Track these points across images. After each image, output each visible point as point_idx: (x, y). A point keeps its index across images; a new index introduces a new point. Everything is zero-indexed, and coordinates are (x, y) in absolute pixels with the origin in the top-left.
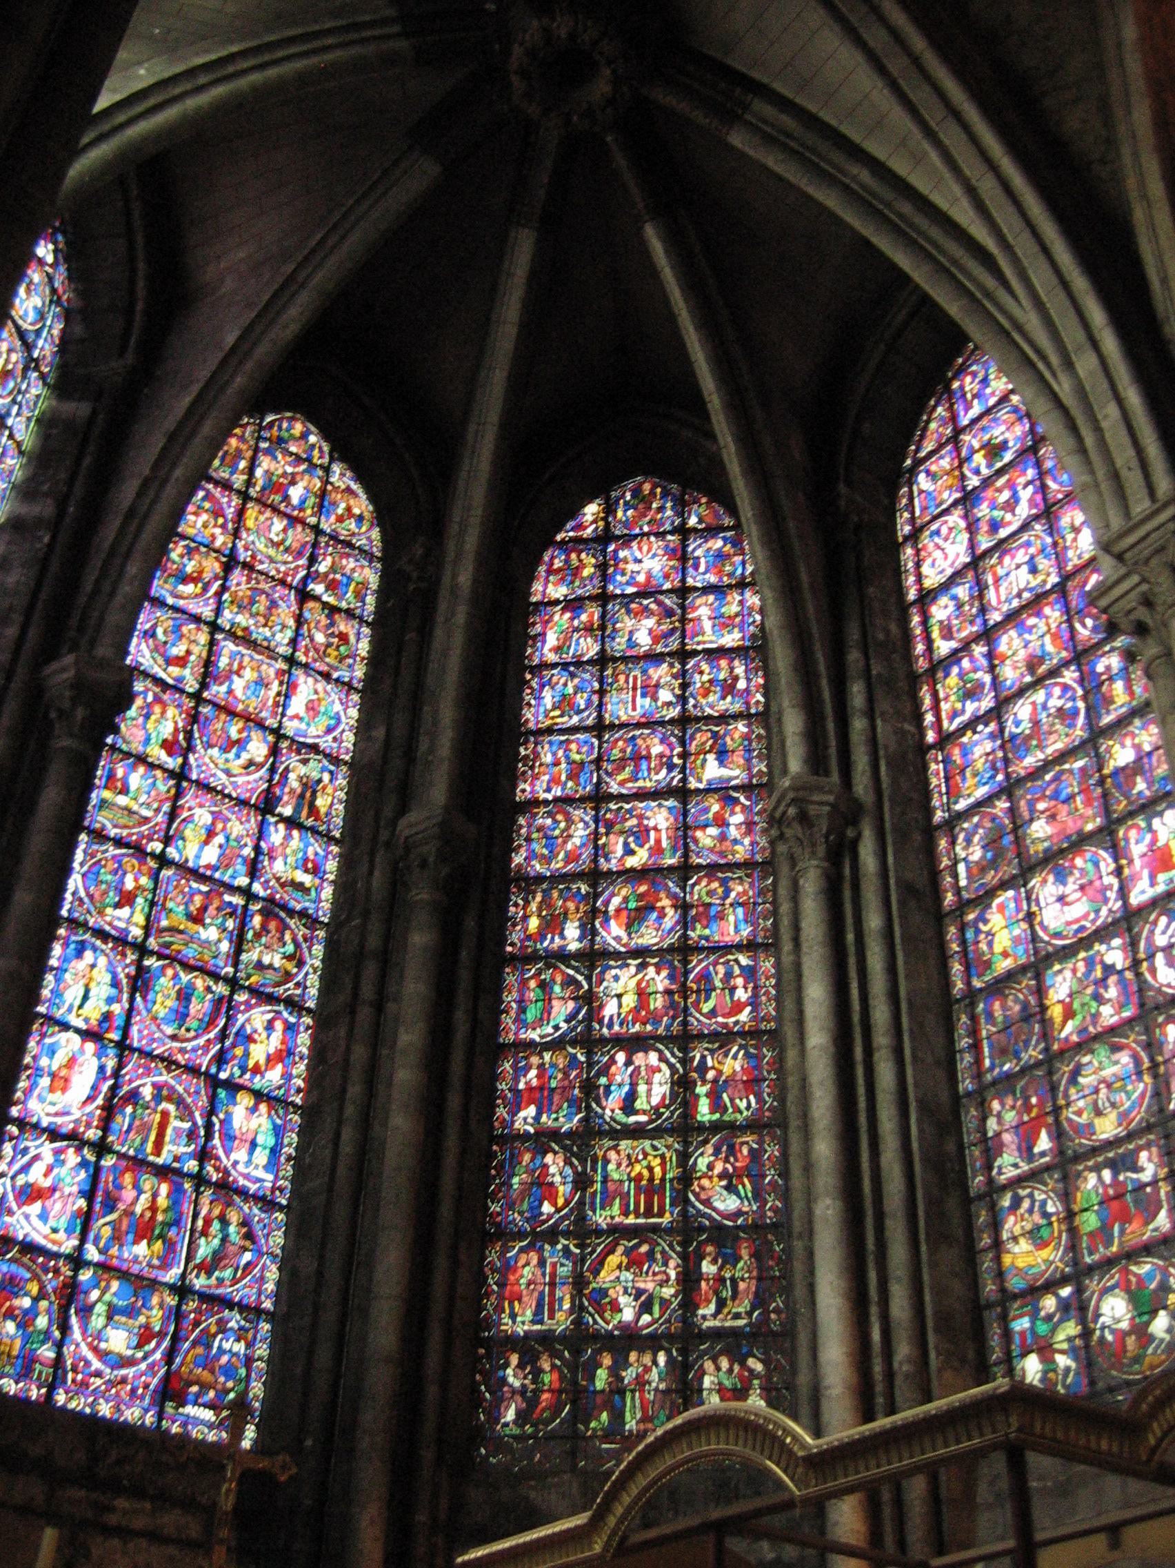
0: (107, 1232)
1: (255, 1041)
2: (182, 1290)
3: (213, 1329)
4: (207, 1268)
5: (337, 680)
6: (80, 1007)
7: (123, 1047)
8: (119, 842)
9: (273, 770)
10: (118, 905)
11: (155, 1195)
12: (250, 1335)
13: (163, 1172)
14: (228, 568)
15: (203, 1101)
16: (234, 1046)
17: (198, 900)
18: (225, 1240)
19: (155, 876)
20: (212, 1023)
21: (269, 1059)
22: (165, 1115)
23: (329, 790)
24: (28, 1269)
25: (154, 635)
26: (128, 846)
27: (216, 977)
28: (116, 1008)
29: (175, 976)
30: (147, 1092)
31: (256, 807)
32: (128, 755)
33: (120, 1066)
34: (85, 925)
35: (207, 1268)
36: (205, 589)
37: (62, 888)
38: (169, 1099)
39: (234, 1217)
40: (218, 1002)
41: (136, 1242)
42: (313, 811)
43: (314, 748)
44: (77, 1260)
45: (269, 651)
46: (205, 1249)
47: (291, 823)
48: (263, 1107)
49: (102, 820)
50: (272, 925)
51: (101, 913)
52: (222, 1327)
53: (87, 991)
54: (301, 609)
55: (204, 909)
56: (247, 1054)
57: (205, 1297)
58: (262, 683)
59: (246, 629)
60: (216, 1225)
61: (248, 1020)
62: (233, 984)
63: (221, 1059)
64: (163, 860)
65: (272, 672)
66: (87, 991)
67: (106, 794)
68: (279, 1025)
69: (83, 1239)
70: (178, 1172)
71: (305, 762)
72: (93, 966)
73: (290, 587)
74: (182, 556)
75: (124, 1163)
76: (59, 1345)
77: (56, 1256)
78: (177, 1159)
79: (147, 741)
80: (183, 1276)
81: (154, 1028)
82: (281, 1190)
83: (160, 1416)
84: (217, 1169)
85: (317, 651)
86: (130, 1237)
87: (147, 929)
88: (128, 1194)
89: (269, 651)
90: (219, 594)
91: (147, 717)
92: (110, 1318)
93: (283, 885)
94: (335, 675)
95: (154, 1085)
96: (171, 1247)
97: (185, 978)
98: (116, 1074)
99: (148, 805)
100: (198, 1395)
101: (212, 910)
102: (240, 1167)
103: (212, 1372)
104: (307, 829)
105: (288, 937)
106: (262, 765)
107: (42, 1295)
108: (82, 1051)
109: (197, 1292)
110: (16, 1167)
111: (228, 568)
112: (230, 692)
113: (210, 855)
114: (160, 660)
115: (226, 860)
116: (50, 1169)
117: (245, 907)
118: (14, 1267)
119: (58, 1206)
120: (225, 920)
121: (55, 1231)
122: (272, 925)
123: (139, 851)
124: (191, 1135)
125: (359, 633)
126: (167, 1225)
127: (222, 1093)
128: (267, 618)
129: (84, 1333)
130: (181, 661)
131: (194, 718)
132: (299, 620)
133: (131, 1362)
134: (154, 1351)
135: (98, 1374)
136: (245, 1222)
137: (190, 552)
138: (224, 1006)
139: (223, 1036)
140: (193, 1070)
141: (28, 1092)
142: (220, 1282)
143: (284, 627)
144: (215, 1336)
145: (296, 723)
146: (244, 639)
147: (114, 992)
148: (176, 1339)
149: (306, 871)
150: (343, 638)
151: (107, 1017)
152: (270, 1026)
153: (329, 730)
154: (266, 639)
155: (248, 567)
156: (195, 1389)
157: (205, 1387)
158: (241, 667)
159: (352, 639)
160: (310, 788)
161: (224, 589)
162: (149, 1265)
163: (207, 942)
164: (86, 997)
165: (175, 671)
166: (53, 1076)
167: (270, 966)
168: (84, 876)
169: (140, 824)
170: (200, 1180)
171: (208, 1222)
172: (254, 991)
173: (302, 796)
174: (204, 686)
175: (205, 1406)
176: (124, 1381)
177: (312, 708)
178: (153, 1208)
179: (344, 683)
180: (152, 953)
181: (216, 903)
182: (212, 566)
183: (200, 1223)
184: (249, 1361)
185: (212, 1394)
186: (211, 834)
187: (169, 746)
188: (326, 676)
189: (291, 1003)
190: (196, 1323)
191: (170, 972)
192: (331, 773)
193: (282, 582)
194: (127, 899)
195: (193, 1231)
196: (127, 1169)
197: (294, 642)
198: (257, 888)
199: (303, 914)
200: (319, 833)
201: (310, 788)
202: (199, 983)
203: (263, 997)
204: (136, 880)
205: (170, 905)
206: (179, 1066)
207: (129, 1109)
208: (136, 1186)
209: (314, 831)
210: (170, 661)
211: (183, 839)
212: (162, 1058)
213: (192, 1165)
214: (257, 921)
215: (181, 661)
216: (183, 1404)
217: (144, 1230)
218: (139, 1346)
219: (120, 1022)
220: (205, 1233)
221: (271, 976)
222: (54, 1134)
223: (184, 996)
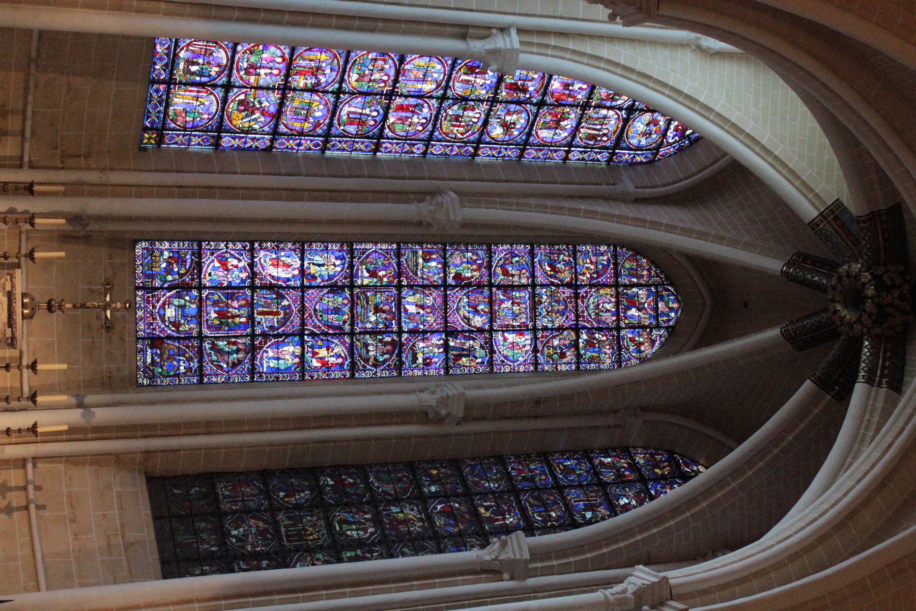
0: (216, 297)
1: (328, 350)
2: (201, 337)
3: (187, 355)
4: (214, 347)
5: (536, 357)
6: (314, 264)
7: (303, 288)
8: (399, 264)
9: (471, 332)
10: (368, 271)
11: (239, 316)
12: (189, 373)
13: (251, 317)
14: (569, 285)
15: (290, 330)
16: (322, 340)
17: (386, 308)
18: (229, 353)
19: (388, 285)
20: (329, 327)
21: (322, 359)
22: (278, 313)
23: (473, 364)
24: (190, 267)
25: (513, 257)
26: (399, 268)
27: (352, 324)
28: (319, 280)
29: (346, 305)
30: (285, 303)
31: (446, 327)
32: (445, 258)
33: (294, 288)
34: (352, 258)
35: (214, 347)
36: (551, 276)
37: (366, 242)
38: (285, 314)
39: (241, 356)
40: (340, 328)
41: (215, 312)
42: (458, 357)
43: (492, 352)
44: (200, 288)
45: (534, 318)
46: (222, 344)
47: (446, 346)
48: (297, 360)
49: (407, 254)
50: (389, 347)
51: (361, 263)
52: (190, 359)
53: (323, 265)
54: (567, 329)
55: (384, 312)
56: (320, 347)
57: (200, 348)
58: (515, 316)
59: (541, 303)
60: (235, 348)
61: (337, 344)
62: (352, 334)
63: (312, 334)
64: (399, 287)
65: (524, 320)
66: (323, 265)
67: (420, 252)
68: (340, 360)
69: (209, 288)
70: (253, 326)
71: (482, 347)
72: (334, 265)
73: (577, 320)
74: (564, 261)
75: (249, 299)
76: (162, 288)
77: (200, 279)
78: (259, 323)
79: (456, 266)
80: (207, 337)
81: (316, 300)
82: (261, 376)
83: (143, 339)
84: (260, 343)
85: (548, 342)
86: (217, 309)
87: (362, 286)
88: (235, 304)
89: (534, 318)
90: (553, 284)
91: (468, 262)
92: (179, 306)
93: (411, 348)
94: (539, 355)
95: (289, 305)
96: (218, 328)
97: (346, 309)
98: (288, 287)
99: (423, 273)
100: (156, 354)
101: (384, 315)
102: (265, 355)
103: (168, 358)
104: (447, 355)
105: (386, 356)
106: (470, 325)
107: (181, 276)
108: (294, 269)
109: (201, 345)
110: (233, 252)
111: (569, 285)
112: (502, 301)
113: (412, 309)
114: (501, 262)
115: (411, 317)
116: (236, 267)
117: (392, 332)
118: (189, 261)
119: (221, 274)
120: (383, 323)
121: (210, 275)
122: (389, 347)
123: (399, 275)
124: (272, 328)
125: (570, 363)
126: (228, 325)
127: (297, 338)
128: (552, 311)
129: (170, 297)
130: (506, 273)
131: (480, 286)
132: (561, 329)
133: (163, 321)
134: (170, 329)
135: (154, 307)
136: (240, 362)
137: (567, 263)
138: (339, 332)
139: (326, 334)
140: (303, 324)
141: (266, 249)
142: (209, 355)
143: (552, 322)
144: (184, 356)
145: (501, 339)
146: (535, 303)
147: (326, 278)
148: (178, 339)
149: (424, 360)
150: (563, 355)
151: (314, 278)
152: (338, 356)
153: (506, 357)
154: (540, 314)
155: (577, 296)
156: (159, 352)
157: (161, 356)
158: (519, 304)
159: (565, 360)
160: (470, 353)
161: (558, 286)
162: (207, 320)
163: (368, 317)
164: (319, 265)
165: (499, 270)
166: (278, 259)
167: (368, 351)
168: (375, 251)
169: (412, 272)
170: (253, 336)
171: (235, 343)
172: (352, 343)
173: (463, 350)
174: (499, 287)
175: (152, 358)
176: (154, 319)
177: (513, 345)
178: (233, 317)
179: (536, 361)
180: (352, 291)
181: (389, 317)
182: (567, 276)
183: (233, 340)
184: (177, 375)
185: (158, 360)
186: (422, 307)
187: (458, 276)
188: (535, 350)
189: (353, 365)
190: (188, 347)
191: (346, 302)
192: (483, 363)
193: (577, 316)
194: (373, 274)
195: (229, 337)
196: (247, 301)
197: (545, 329)
198: (405, 336)
199: (401, 363)
200: (447, 363)
201: (470, 353)
202: (346, 317)
203: (351, 349)
204: (384, 276)
205: (379, 296)
206: (303, 315)
207: (274, 296)
208: (241, 307)
209: (447, 359)
210: (502, 267)
211: (414, 294)
212: (303, 306)
213: (258, 331)
214: (388, 339)
215: (506, 273)
216: (152, 348)
217: (222, 315)
218: (170, 322)
219: (313, 283)
220: (229, 343)
221: (364, 351)
222: (252, 265)
223: (337, 311)
